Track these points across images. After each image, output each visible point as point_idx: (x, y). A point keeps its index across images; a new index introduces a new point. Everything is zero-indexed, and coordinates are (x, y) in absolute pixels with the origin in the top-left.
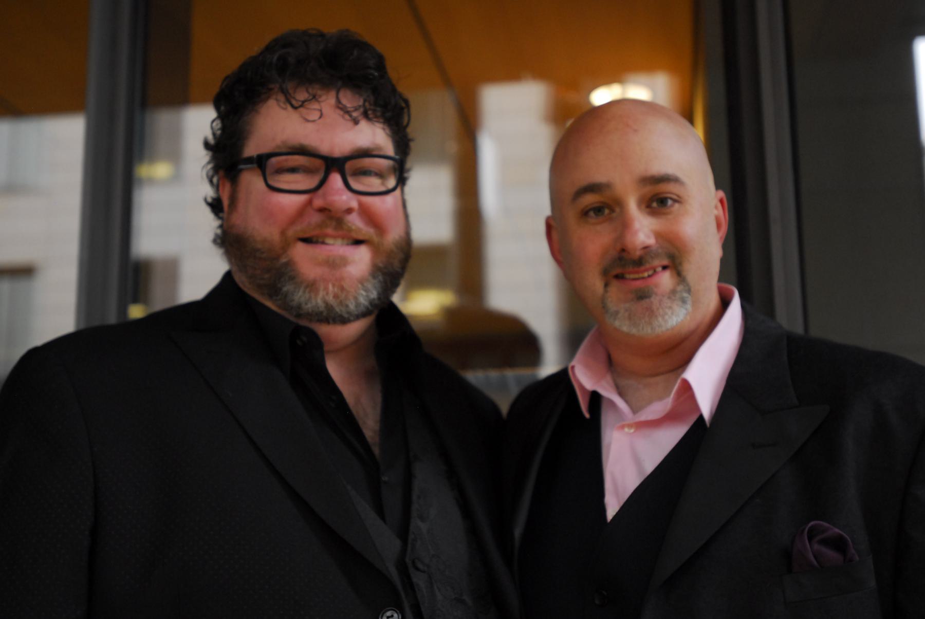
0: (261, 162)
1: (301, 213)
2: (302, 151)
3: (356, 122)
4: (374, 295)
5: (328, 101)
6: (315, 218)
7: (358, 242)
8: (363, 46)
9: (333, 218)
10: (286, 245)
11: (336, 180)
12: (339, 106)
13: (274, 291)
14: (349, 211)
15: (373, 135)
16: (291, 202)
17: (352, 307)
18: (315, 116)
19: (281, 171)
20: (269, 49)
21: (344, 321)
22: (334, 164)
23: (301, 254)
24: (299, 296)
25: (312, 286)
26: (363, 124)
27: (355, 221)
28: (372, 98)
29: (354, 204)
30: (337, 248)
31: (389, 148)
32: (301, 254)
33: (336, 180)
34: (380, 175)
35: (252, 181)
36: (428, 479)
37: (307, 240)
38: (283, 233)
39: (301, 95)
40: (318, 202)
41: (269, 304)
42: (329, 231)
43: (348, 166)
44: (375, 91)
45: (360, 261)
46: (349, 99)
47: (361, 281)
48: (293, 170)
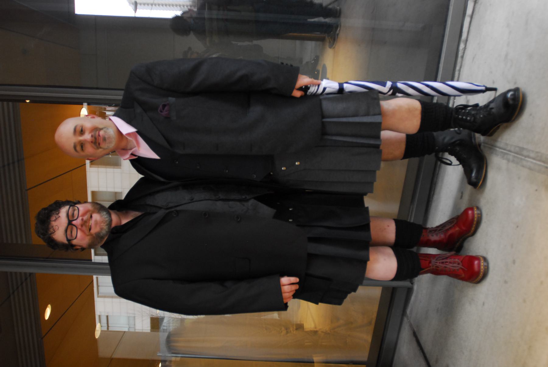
0: (69, 240)
1: (82, 231)
2: (66, 231)
3: (59, 217)
4: (105, 213)
5: (54, 224)
6: (84, 228)
7: (91, 217)
8: (39, 214)
9: (84, 223)
10: (91, 235)
11: (74, 222)
12: (55, 221)
13: (102, 238)
14: (82, 219)
15: (64, 211)
16: (80, 234)
17: (107, 219)
18: (57, 227)
19: (72, 236)
20: (39, 237)
21: (111, 221)
22: (70, 223)
23: (93, 231)
24: (104, 232)
25: (102, 229)
26: (61, 215)
27: (85, 218)
28: (54, 212)
29: (80, 218)
30: (92, 222)
31: (67, 207)
32: (93, 231)
33: (74, 222)
34: (74, 210)
35: (75, 242)
36: (150, 201)
37: (90, 230)
38: (88, 235)
39: (52, 230)
40: (80, 227)
41: (106, 239)
42: (87, 224)
43: (71, 219)
44: (51, 211)
45: (96, 217)
46: (53, 218)
47: (101, 216)
48: (71, 232)
